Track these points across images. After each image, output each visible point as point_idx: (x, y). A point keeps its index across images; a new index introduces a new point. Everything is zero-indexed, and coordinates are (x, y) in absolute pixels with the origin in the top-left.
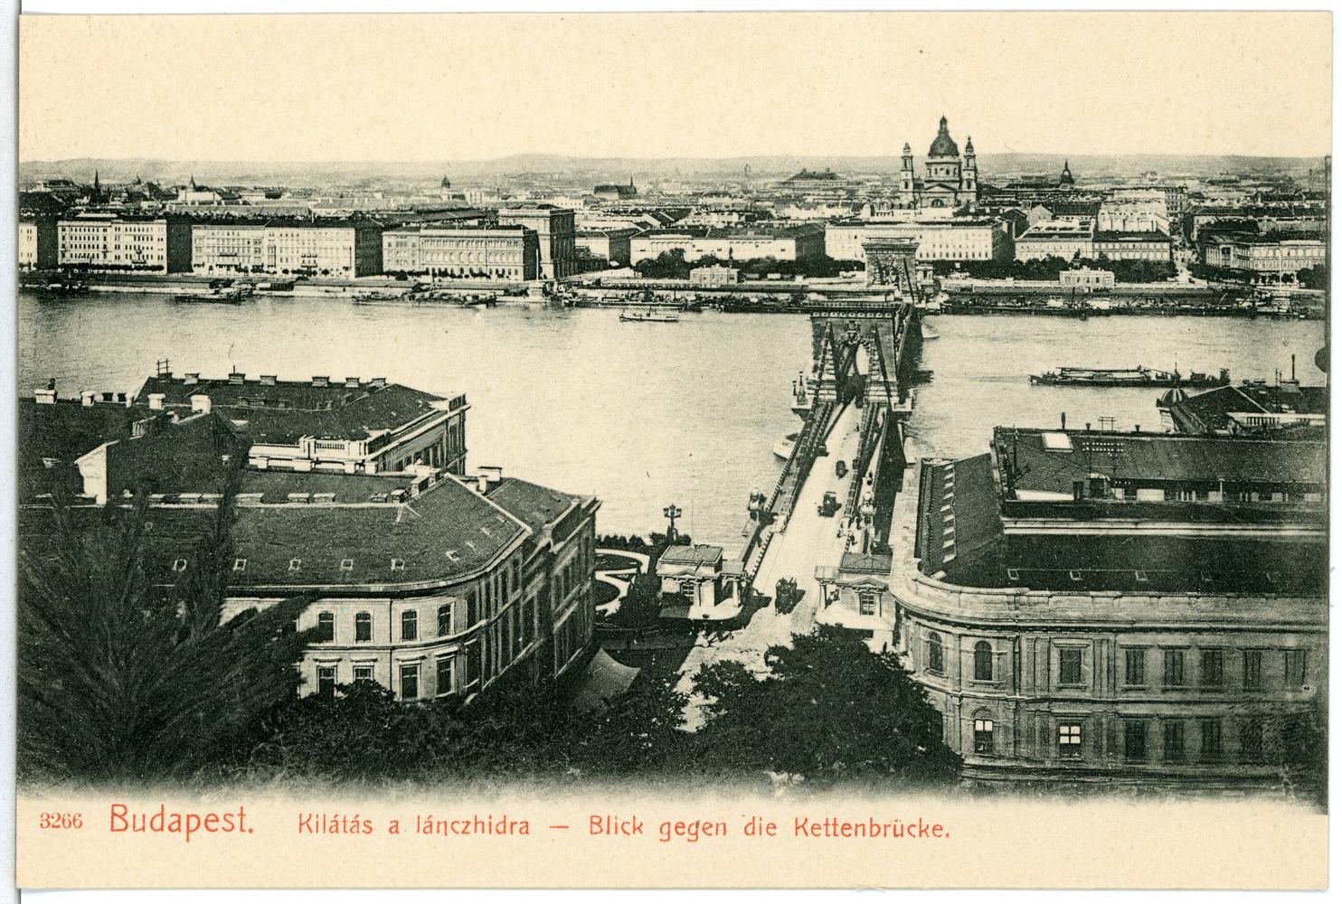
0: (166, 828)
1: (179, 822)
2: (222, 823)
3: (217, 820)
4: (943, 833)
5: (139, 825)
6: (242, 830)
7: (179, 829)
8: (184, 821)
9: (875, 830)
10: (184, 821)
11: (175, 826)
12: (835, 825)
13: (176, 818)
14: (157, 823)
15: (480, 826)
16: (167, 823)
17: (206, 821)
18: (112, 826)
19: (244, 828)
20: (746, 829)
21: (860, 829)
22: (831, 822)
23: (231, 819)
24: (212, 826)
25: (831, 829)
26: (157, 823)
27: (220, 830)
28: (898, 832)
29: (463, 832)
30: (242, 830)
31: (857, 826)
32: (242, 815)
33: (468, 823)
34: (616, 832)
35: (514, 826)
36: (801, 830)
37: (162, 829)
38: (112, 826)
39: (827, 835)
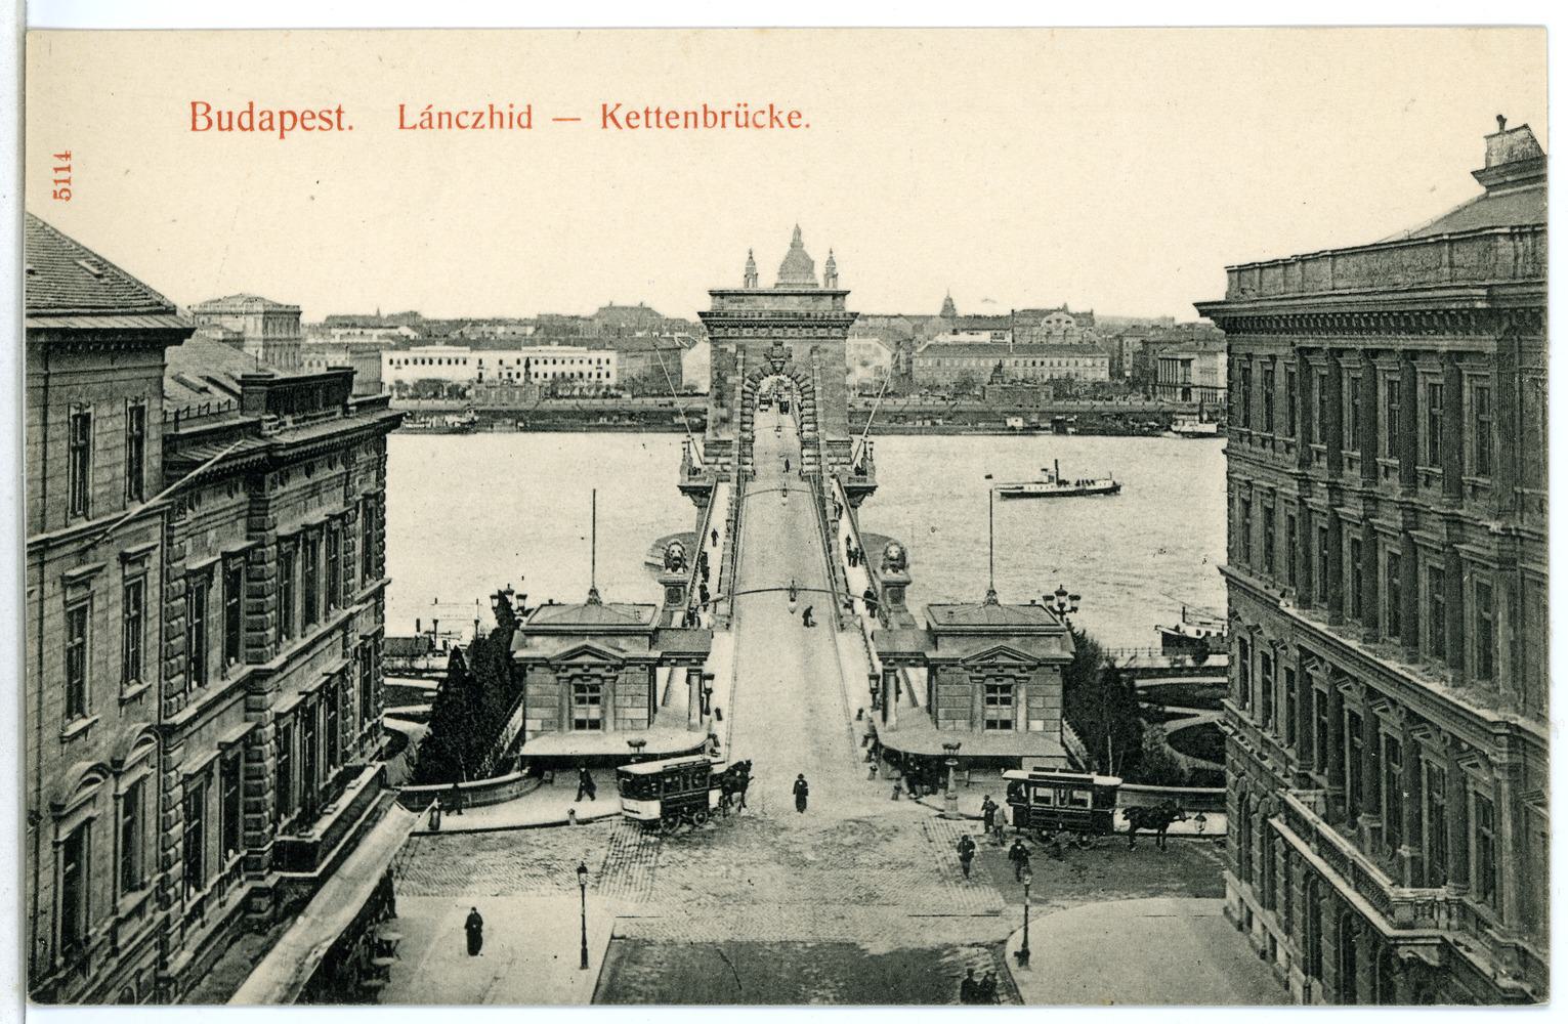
1: (271, 119)
2: (319, 122)
3: (314, 116)
4: (803, 121)
5: (225, 124)
6: (340, 128)
7: (271, 128)
9: (710, 117)
12: (658, 112)
13: (267, 115)
14: (246, 122)
17: (303, 118)
18: (194, 121)
21: (691, 118)
22: (653, 109)
24: (309, 124)
25: (653, 118)
26: (246, 124)
28: (742, 120)
29: (474, 126)
30: (340, 128)
31: (686, 114)
32: (339, 112)
33: (481, 114)
36: (609, 121)
37: (252, 128)
38: (194, 121)
39: (647, 126)
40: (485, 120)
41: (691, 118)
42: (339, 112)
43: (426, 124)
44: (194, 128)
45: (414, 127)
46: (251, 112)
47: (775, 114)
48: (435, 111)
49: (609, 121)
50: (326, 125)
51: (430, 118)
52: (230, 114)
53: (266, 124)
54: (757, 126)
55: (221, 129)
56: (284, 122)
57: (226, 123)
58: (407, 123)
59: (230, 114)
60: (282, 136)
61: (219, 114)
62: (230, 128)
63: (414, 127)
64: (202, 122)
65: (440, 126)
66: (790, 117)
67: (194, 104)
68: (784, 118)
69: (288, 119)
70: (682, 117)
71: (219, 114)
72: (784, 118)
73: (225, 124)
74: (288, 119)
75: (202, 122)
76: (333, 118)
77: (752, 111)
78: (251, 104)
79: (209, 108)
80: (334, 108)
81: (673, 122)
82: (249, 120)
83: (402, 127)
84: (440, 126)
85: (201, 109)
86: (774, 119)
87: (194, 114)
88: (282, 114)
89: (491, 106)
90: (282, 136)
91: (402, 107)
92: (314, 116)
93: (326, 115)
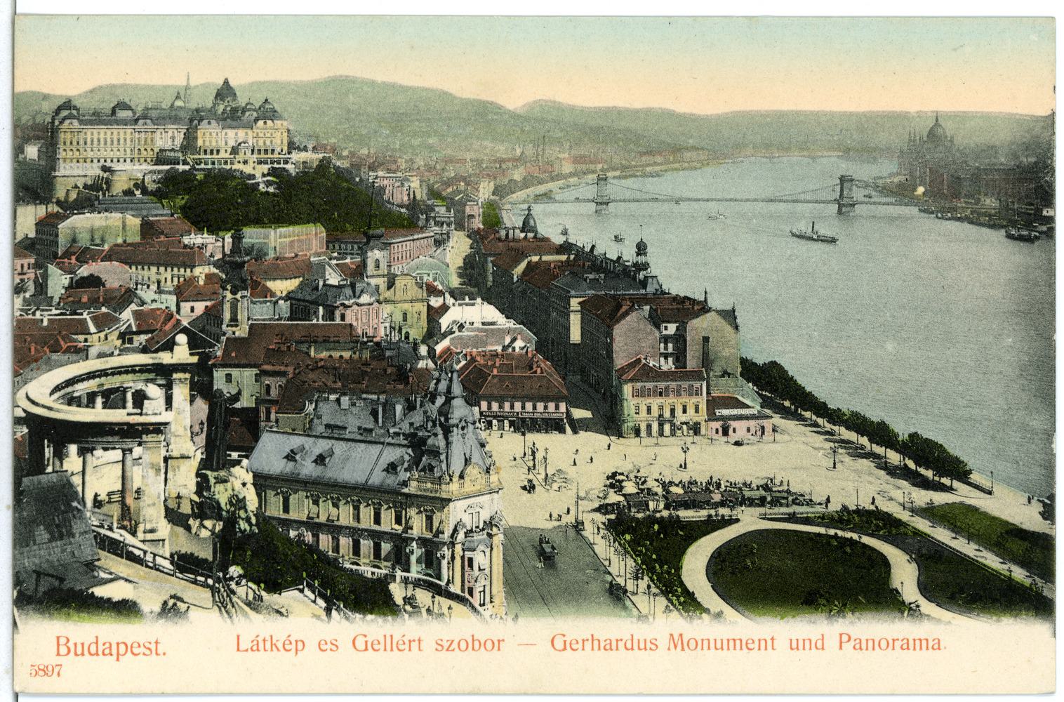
0: (100, 652)
2: (142, 650)
3: (139, 646)
5: (79, 652)
6: (157, 654)
11: (107, 651)
14: (93, 649)
15: (596, 643)
16: (101, 648)
17: (132, 647)
19: (159, 652)
20: (304, 645)
24: (136, 650)
26: (93, 649)
30: (157, 654)
32: (157, 643)
34: (741, 649)
37: (97, 654)
40: (588, 645)
41: (763, 643)
42: (157, 643)
43: (255, 648)
44: (58, 654)
45: (247, 650)
46: (97, 643)
47: (274, 641)
48: (260, 639)
50: (148, 652)
52: (83, 644)
53: (107, 651)
54: (399, 650)
55: (76, 654)
58: (240, 649)
59: (83, 644)
60: (118, 659)
61: (75, 644)
62: (83, 654)
63: (247, 650)
64: (63, 650)
66: (284, 644)
67: (58, 638)
68: (280, 645)
69: (122, 648)
70: (757, 643)
71: (75, 644)
72: (280, 645)
73: (79, 652)
74: (122, 648)
75: (63, 650)
76: (153, 647)
77: (370, 639)
78: (97, 637)
79: (68, 641)
80: (155, 640)
83: (238, 650)
85: (63, 641)
87: (58, 645)
88: (118, 644)
89: (592, 636)
90: (118, 659)
91: (238, 637)
92: (139, 646)
93: (147, 645)
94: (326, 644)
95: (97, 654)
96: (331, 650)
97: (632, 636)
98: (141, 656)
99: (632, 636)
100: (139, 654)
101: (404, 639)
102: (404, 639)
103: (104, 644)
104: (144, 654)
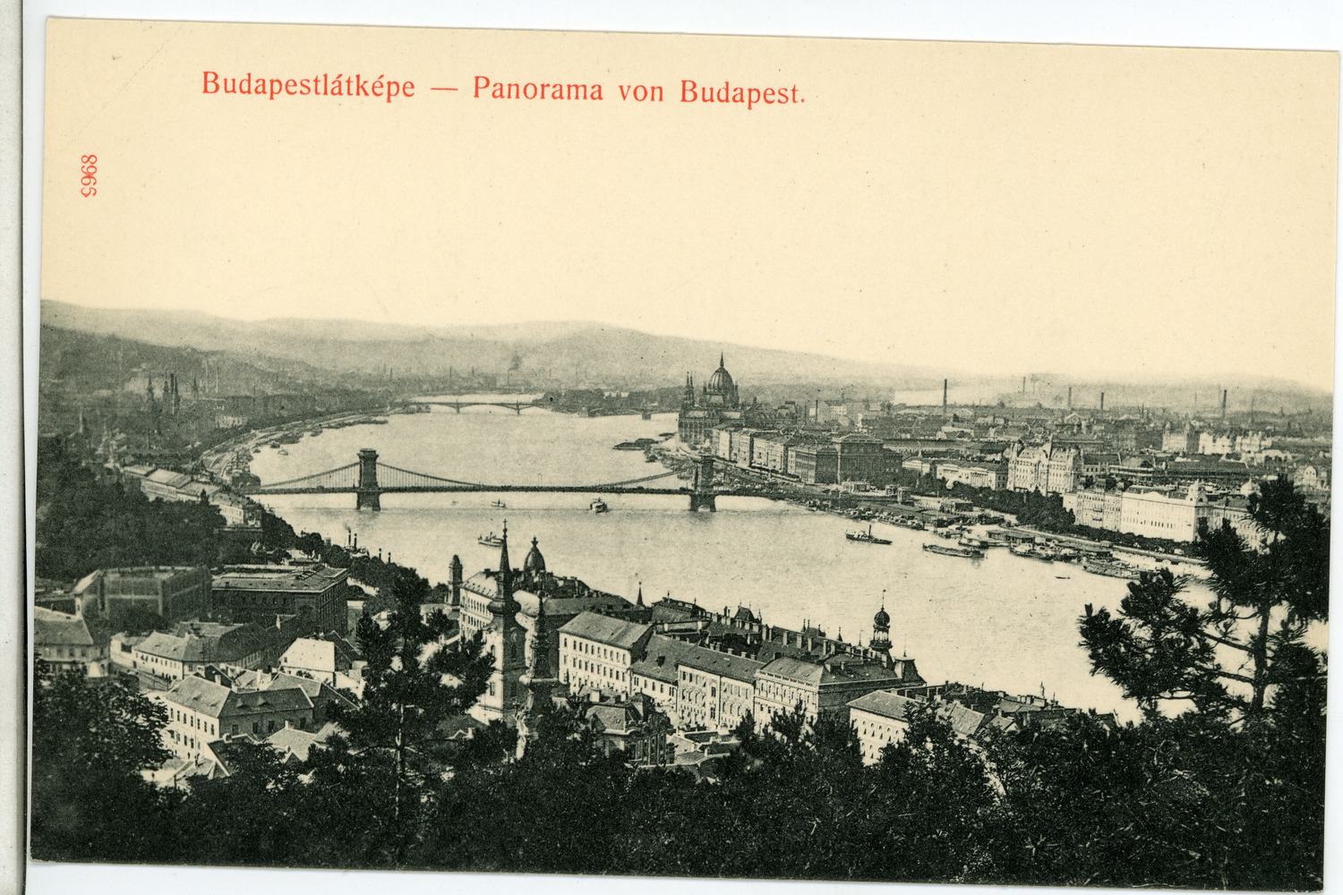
0: (730, 99)
1: (742, 93)
2: (777, 96)
7: (742, 100)
8: (746, 93)
10: (746, 93)
11: (738, 98)
17: (765, 94)
23: (786, 93)
26: (723, 96)
27: (776, 102)
35: (546, 89)
37: (727, 100)
42: (794, 90)
47: (361, 83)
49: (361, 91)
51: (501, 89)
52: (712, 89)
53: (738, 98)
56: (749, 97)
57: (710, 97)
59: (712, 89)
65: (569, 98)
66: (374, 87)
68: (368, 88)
69: (754, 95)
74: (754, 95)
76: (789, 94)
80: (790, 88)
81: (378, 91)
82: (729, 95)
84: (569, 98)
86: (360, 88)
90: (750, 108)
94: (774, 93)
95: (727, 100)
96: (779, 101)
97: (727, 83)
98: (776, 103)
99: (727, 83)
100: (772, 102)
101: (382, 80)
102: (382, 80)
103: (735, 90)
104: (779, 101)
